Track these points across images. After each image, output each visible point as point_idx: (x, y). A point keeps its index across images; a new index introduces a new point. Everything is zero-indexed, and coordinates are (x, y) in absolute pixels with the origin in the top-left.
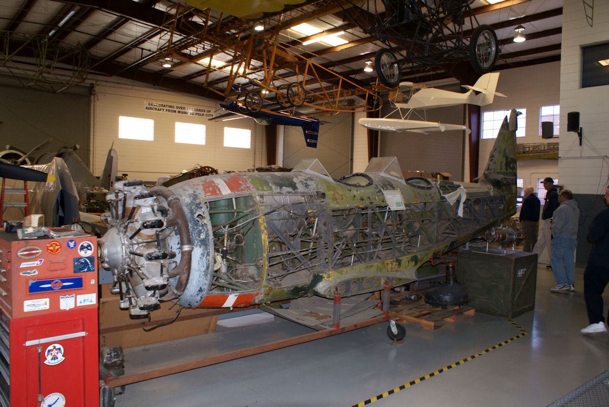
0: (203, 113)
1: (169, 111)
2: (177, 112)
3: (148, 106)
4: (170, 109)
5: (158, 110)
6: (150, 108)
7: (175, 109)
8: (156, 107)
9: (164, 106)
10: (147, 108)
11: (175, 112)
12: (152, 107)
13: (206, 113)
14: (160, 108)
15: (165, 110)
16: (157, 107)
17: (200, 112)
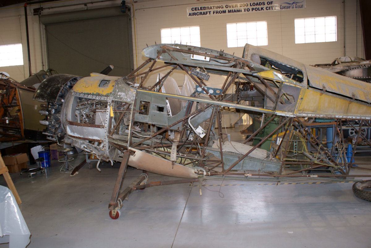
0: (262, 6)
1: (217, 12)
2: (227, 11)
3: (191, 12)
4: (219, 10)
5: (204, 14)
6: (194, 14)
7: (224, 9)
8: (201, 11)
9: (211, 8)
10: (190, 14)
11: (224, 12)
12: (196, 12)
13: (266, 5)
14: (205, 11)
15: (212, 13)
16: (203, 11)
17: (257, 7)
